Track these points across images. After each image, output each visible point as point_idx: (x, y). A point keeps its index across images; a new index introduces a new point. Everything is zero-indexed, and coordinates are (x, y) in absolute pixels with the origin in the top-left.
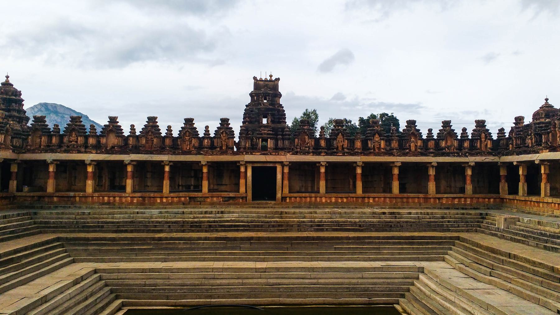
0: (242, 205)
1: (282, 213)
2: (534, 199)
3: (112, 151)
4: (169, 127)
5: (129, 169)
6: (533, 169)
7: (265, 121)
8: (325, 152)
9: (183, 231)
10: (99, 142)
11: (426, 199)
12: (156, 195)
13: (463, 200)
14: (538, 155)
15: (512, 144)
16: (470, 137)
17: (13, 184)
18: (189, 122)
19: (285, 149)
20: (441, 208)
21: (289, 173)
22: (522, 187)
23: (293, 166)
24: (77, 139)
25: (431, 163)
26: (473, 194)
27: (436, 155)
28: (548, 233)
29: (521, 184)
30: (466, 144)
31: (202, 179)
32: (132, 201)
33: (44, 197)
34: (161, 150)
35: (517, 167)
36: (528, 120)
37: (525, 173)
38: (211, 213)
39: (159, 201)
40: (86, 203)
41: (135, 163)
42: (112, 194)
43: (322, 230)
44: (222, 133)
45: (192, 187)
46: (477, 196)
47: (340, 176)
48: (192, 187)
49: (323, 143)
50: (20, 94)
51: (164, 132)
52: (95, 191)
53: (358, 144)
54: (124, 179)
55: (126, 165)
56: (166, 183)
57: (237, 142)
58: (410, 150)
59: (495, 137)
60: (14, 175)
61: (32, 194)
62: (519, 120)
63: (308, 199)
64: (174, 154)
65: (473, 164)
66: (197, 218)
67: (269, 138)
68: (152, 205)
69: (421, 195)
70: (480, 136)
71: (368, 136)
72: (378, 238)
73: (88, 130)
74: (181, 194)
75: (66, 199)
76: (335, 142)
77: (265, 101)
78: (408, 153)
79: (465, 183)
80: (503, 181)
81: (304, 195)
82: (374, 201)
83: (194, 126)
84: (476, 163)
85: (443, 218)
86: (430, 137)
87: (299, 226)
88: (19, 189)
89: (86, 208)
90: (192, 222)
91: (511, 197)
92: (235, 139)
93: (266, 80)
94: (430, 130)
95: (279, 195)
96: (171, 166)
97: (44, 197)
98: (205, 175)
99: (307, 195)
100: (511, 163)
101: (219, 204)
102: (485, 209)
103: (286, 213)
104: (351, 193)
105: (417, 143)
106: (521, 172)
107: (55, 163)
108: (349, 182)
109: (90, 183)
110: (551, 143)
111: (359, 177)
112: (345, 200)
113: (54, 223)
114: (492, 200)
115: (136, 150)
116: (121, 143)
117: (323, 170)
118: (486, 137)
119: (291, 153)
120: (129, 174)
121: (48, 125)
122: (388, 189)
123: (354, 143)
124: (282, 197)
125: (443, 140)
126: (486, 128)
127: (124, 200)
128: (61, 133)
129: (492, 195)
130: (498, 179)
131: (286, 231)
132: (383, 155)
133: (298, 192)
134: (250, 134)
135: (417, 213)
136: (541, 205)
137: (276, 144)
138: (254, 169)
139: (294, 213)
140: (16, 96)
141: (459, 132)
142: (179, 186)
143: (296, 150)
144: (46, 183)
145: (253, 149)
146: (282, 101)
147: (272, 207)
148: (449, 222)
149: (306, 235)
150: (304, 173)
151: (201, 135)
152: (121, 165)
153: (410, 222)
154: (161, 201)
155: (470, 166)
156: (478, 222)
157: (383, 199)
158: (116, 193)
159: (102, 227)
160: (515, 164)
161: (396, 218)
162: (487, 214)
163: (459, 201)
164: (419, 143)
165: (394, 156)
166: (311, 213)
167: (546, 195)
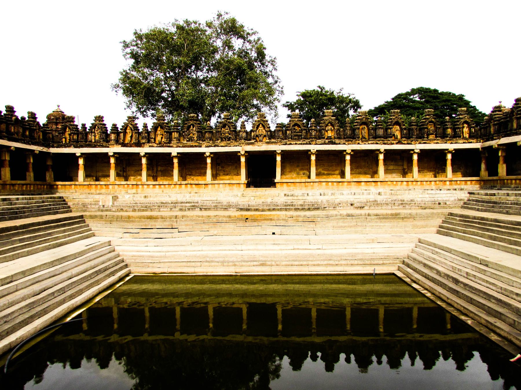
11: (4, 185)
15: (66, 138)
27: (10, 140)
28: (170, 202)
46: (38, 183)
65: (38, 152)
79: (28, 171)
80: (51, 170)
85: (43, 202)
91: (67, 183)
114: (45, 187)
125: (12, 125)
126: (38, 120)
135: (23, 199)
148: (50, 205)
160: (78, 155)
163: (26, 188)
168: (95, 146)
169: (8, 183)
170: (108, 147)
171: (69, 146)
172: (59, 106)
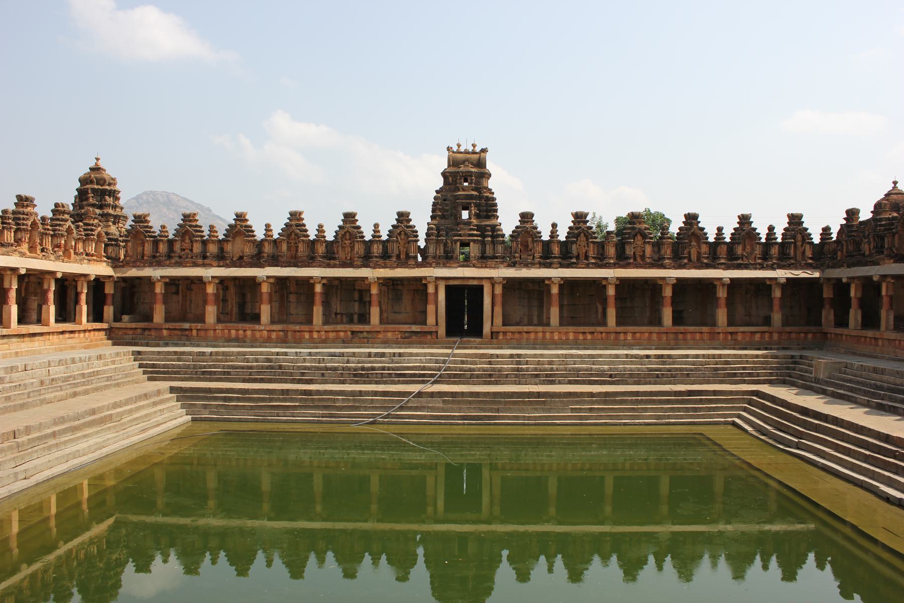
0: (432, 345)
1: (492, 356)
2: (870, 333)
3: (240, 262)
4: (320, 226)
5: (265, 288)
6: (870, 287)
7: (465, 215)
8: (560, 263)
9: (343, 382)
10: (222, 250)
12: (303, 328)
13: (767, 335)
14: (877, 267)
15: (842, 251)
16: (779, 240)
17: (109, 311)
18: (349, 218)
19: (497, 258)
20: (734, 349)
21: (504, 295)
22: (855, 316)
23: (511, 285)
24: (192, 246)
25: (720, 279)
26: (783, 326)
27: (728, 267)
29: (852, 312)
30: (774, 251)
31: (370, 302)
32: (269, 337)
33: (149, 330)
34: (310, 261)
35: (848, 285)
36: (865, 215)
37: (859, 295)
38: (383, 355)
39: (307, 336)
40: (205, 339)
41: (272, 280)
42: (240, 325)
43: (552, 383)
44: (400, 234)
45: (356, 317)
46: (788, 329)
47: (582, 301)
48: (356, 317)
49: (556, 250)
50: (115, 184)
51: (312, 234)
52: (219, 321)
53: (611, 251)
54: (258, 304)
55: (260, 284)
56: (318, 311)
57: (422, 247)
58: (690, 260)
59: (816, 240)
60: (109, 300)
61: (134, 325)
62: (852, 214)
63: (532, 336)
64: (329, 266)
66: (364, 362)
67: (474, 241)
68: (298, 342)
69: (705, 329)
70: (794, 237)
71: (626, 238)
72: (637, 393)
73: (206, 233)
74: (339, 327)
75: (179, 333)
76: (574, 247)
77: (466, 184)
78: (685, 264)
80: (827, 306)
81: (525, 328)
82: (634, 338)
83: (358, 224)
84: (788, 279)
86: (719, 239)
87: (517, 376)
88: (117, 319)
89: (207, 346)
90: (355, 370)
91: (839, 331)
92: (419, 244)
93: (466, 152)
94: (720, 229)
95: (487, 328)
96: (324, 284)
97: (149, 330)
98: (375, 299)
99: (531, 328)
100: (839, 280)
101: (397, 343)
102: (799, 349)
103: (498, 356)
104: (599, 325)
105: (700, 248)
106: (852, 294)
107: (163, 280)
108: (597, 308)
109: (211, 312)
110: (897, 249)
111: (611, 302)
112: (589, 337)
113: (164, 366)
114: (810, 336)
115: (275, 261)
116: (254, 251)
117: (555, 290)
118: (803, 240)
119: (505, 264)
120: (265, 297)
121: (151, 227)
122: (656, 321)
123: (603, 247)
124: (492, 333)
125: (739, 244)
126: (804, 225)
127: (258, 334)
128: (171, 237)
129: (811, 328)
130: (821, 302)
131: (496, 383)
132: (649, 268)
133: (518, 324)
134: (442, 235)
135: (697, 356)
136: (880, 343)
137: (483, 252)
138: (448, 289)
139: (512, 356)
140: (109, 185)
141: (763, 233)
142: (336, 314)
143: (513, 260)
144: (152, 309)
145: (447, 259)
146: (491, 184)
147: (476, 348)
148: (744, 368)
149: (527, 390)
150: (526, 296)
151: (368, 237)
152: (253, 282)
153: (686, 369)
154: (311, 337)
155: (778, 284)
156: (788, 368)
157: (647, 335)
158: (247, 326)
159: (229, 373)
161: (664, 363)
162: (801, 357)
163: (761, 338)
164: (704, 249)
165: (665, 268)
166: (535, 356)
167: (887, 329)
168: (866, 264)
169: (720, 330)
170: (878, 264)
171: (842, 266)
172: (895, 183)
